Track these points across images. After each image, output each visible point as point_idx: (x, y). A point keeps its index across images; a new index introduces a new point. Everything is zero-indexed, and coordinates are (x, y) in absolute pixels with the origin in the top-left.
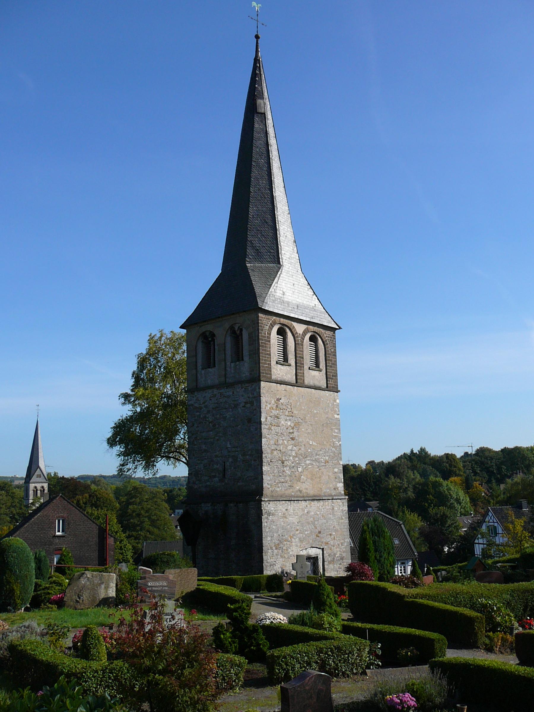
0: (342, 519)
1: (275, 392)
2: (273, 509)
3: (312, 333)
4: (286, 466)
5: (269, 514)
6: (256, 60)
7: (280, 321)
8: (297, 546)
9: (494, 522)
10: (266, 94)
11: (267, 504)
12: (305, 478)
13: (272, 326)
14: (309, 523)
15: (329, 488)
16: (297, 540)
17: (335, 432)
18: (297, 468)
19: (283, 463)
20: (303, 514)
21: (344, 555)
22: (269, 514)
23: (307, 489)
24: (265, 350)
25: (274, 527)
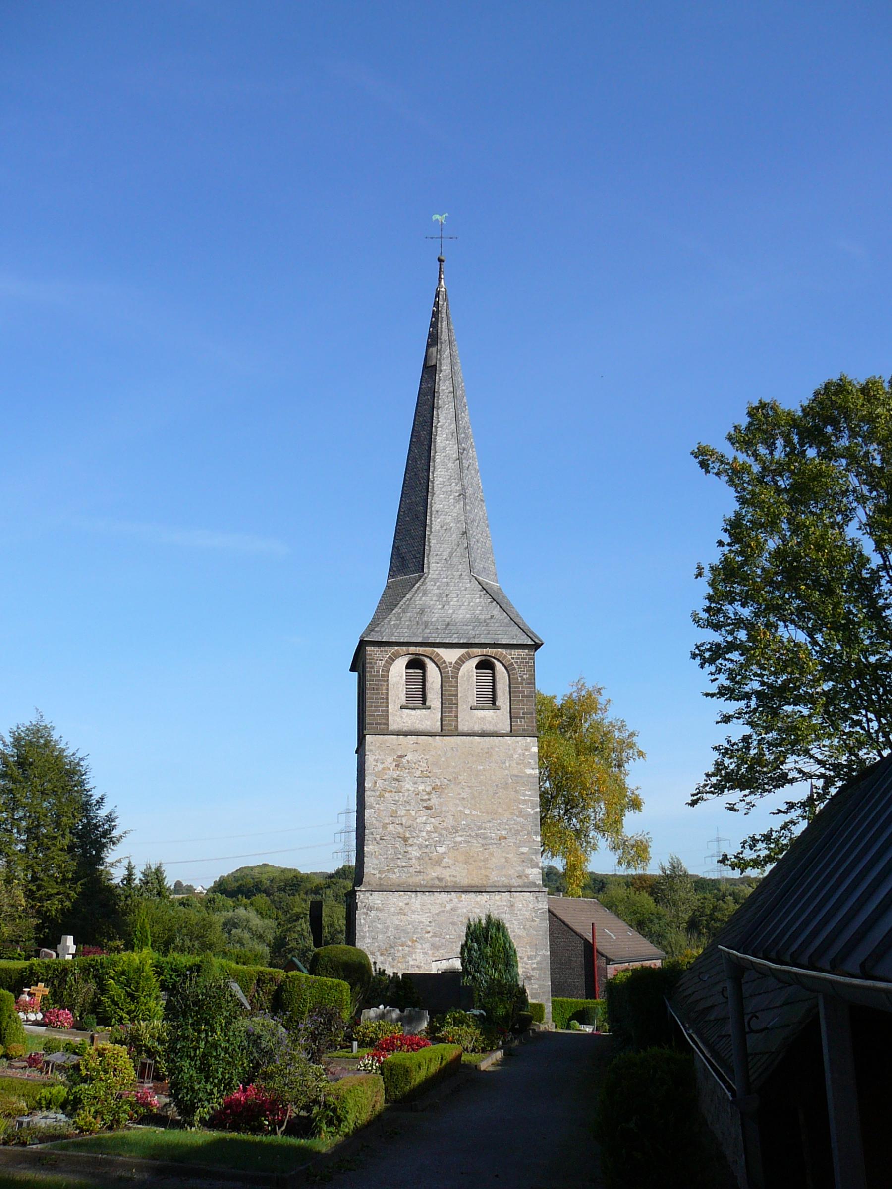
0: (533, 921)
1: (395, 747)
2: (379, 902)
3: (483, 658)
4: (411, 845)
5: (370, 909)
7: (408, 650)
8: (425, 953)
10: (444, 337)
11: (368, 894)
12: (451, 862)
13: (392, 660)
14: (453, 924)
15: (509, 877)
16: (427, 946)
17: (525, 795)
18: (435, 847)
19: (405, 840)
20: (443, 911)
21: (535, 974)
22: (370, 909)
24: (378, 694)
25: (379, 926)
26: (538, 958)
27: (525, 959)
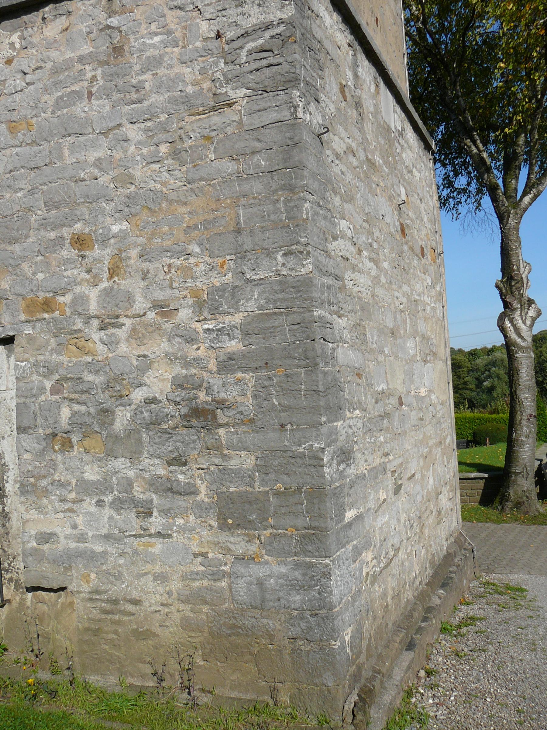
0: (223, 104)
21: (239, 391)
26: (251, 304)
27: (185, 314)
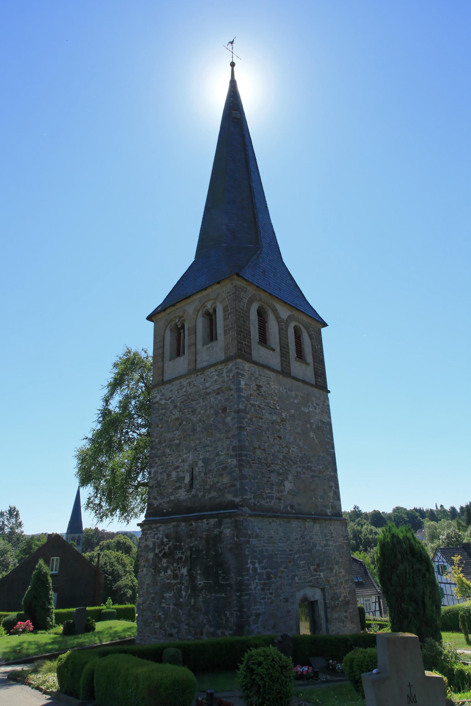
6: (233, 83)
9: (443, 562)
13: (251, 301)
23: (299, 504)
